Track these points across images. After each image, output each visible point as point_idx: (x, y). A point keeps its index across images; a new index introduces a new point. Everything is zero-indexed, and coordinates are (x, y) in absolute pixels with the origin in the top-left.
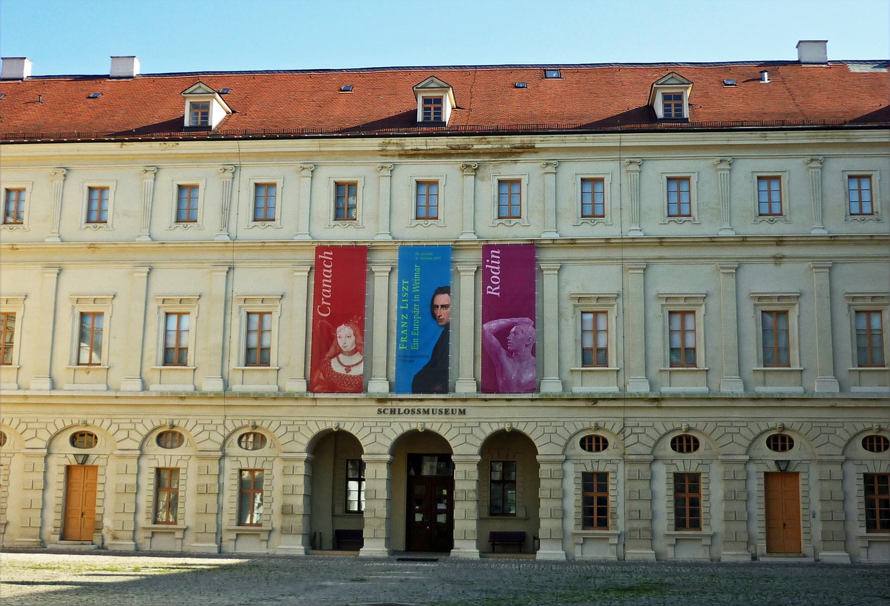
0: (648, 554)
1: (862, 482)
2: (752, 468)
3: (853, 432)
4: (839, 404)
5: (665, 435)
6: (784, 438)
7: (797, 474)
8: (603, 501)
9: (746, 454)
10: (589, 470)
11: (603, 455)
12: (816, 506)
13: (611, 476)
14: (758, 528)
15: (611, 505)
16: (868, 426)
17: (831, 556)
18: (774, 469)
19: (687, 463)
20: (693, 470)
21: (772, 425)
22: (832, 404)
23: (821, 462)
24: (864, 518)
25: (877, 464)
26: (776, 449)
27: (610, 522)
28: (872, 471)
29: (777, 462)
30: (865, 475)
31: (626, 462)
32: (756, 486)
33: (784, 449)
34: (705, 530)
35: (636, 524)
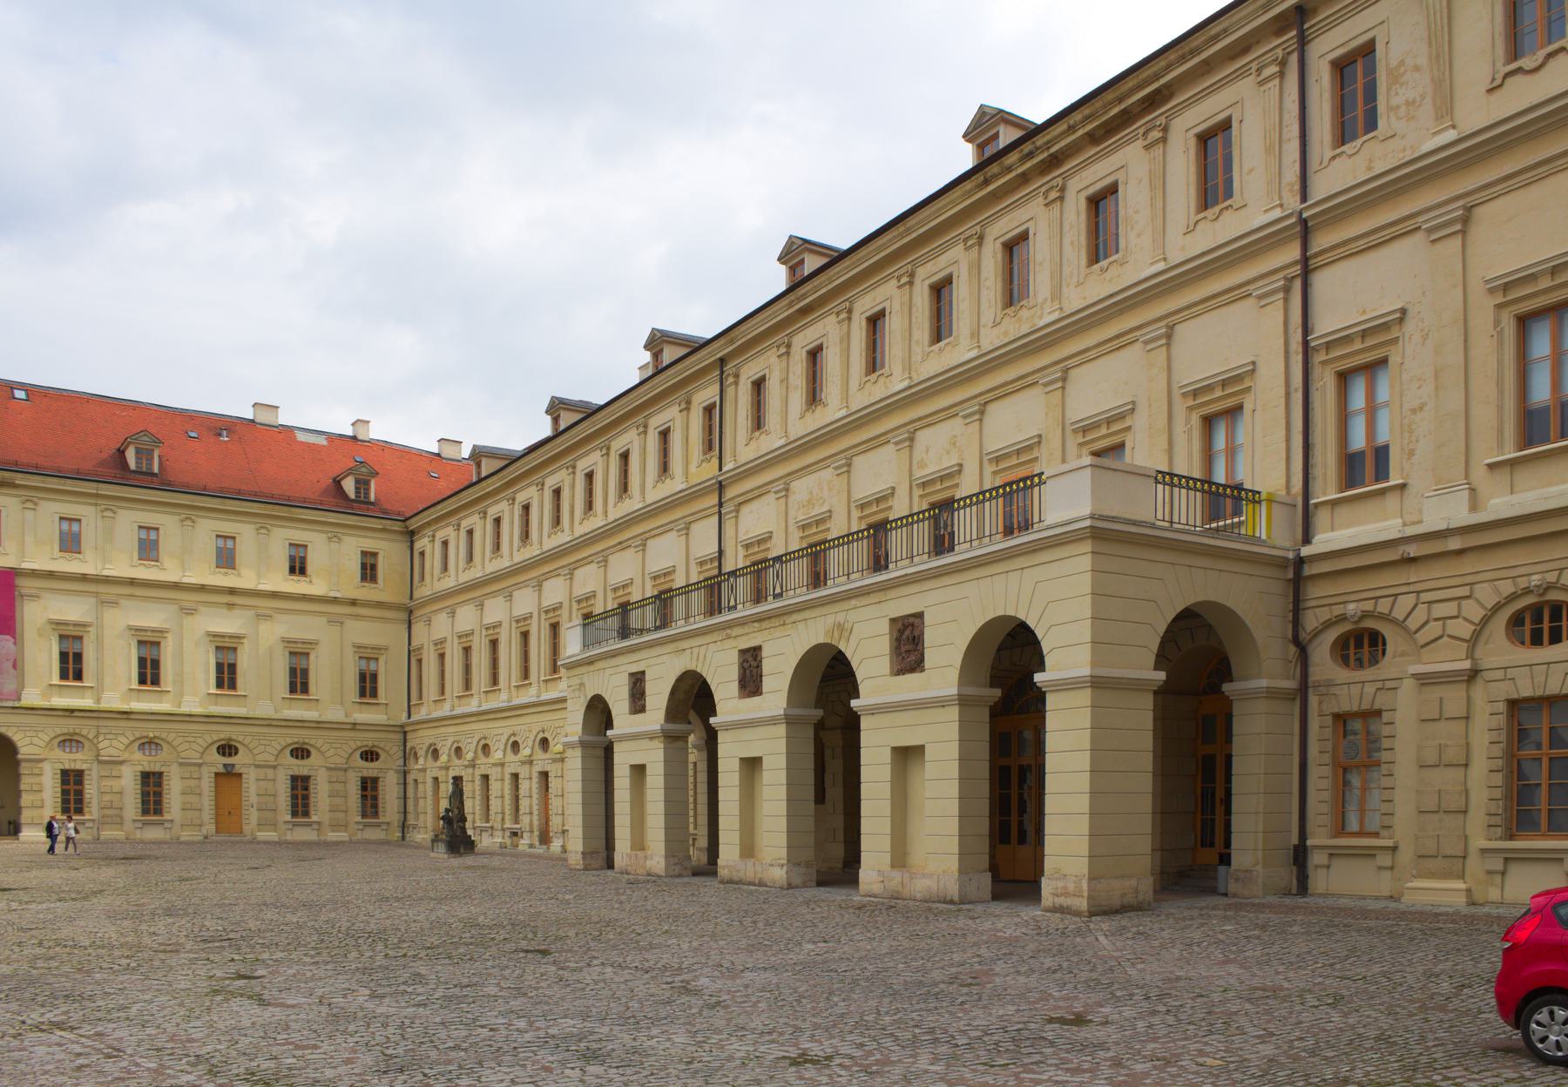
0: (119, 834)
1: (289, 782)
2: (205, 770)
3: (284, 744)
4: (274, 723)
5: (134, 741)
6: (230, 747)
7: (240, 775)
8: (80, 793)
9: (201, 758)
10: (67, 767)
11: (79, 756)
12: (253, 799)
13: (86, 772)
14: (208, 814)
15: (87, 796)
16: (296, 740)
17: (263, 835)
18: (222, 770)
19: (152, 764)
20: (157, 770)
21: (222, 736)
22: (268, 723)
23: (257, 766)
24: (289, 808)
25: (301, 768)
26: (224, 755)
27: (86, 810)
28: (297, 773)
29: (225, 765)
30: (292, 776)
31: (100, 762)
32: (207, 784)
33: (230, 755)
34: (167, 817)
35: (109, 812)
